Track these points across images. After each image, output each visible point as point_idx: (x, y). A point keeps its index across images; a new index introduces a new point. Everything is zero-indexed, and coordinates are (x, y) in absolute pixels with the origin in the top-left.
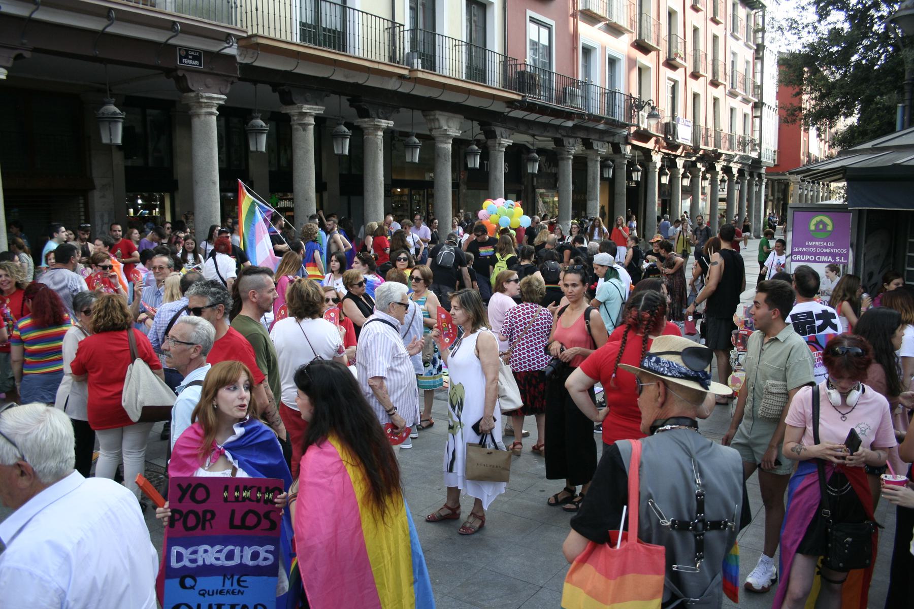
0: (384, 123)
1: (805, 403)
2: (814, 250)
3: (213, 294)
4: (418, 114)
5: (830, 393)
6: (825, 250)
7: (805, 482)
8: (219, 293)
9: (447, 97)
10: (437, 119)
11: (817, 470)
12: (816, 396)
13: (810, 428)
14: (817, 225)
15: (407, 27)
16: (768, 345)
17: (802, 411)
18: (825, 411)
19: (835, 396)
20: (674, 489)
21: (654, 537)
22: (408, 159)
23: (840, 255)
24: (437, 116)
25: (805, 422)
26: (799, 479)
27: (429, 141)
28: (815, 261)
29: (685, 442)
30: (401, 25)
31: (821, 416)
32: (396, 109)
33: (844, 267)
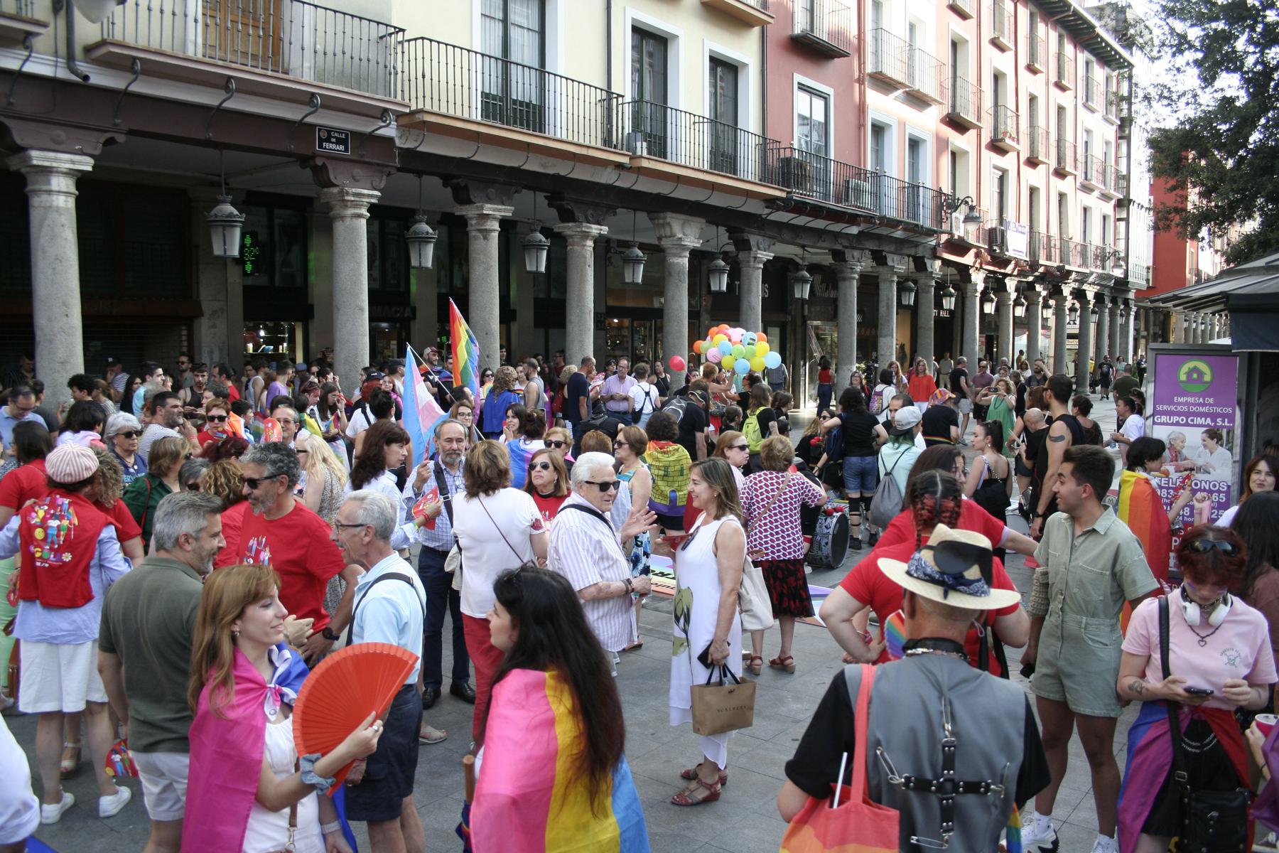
0: (595, 229)
1: (1148, 621)
2: (1185, 408)
3: (274, 462)
4: (642, 217)
5: (1185, 608)
6: (1201, 409)
7: (1151, 733)
8: (281, 461)
9: (682, 193)
10: (669, 224)
11: (1167, 716)
12: (1164, 612)
13: (1157, 656)
14: (1189, 374)
15: (628, 98)
16: (1081, 539)
17: (1145, 633)
18: (1178, 635)
19: (1193, 611)
21: (884, 797)
23: (1223, 416)
24: (668, 220)
25: (1149, 648)
27: (656, 253)
28: (1187, 425)
30: (619, 96)
31: (1171, 639)
32: (611, 210)
33: (1228, 433)
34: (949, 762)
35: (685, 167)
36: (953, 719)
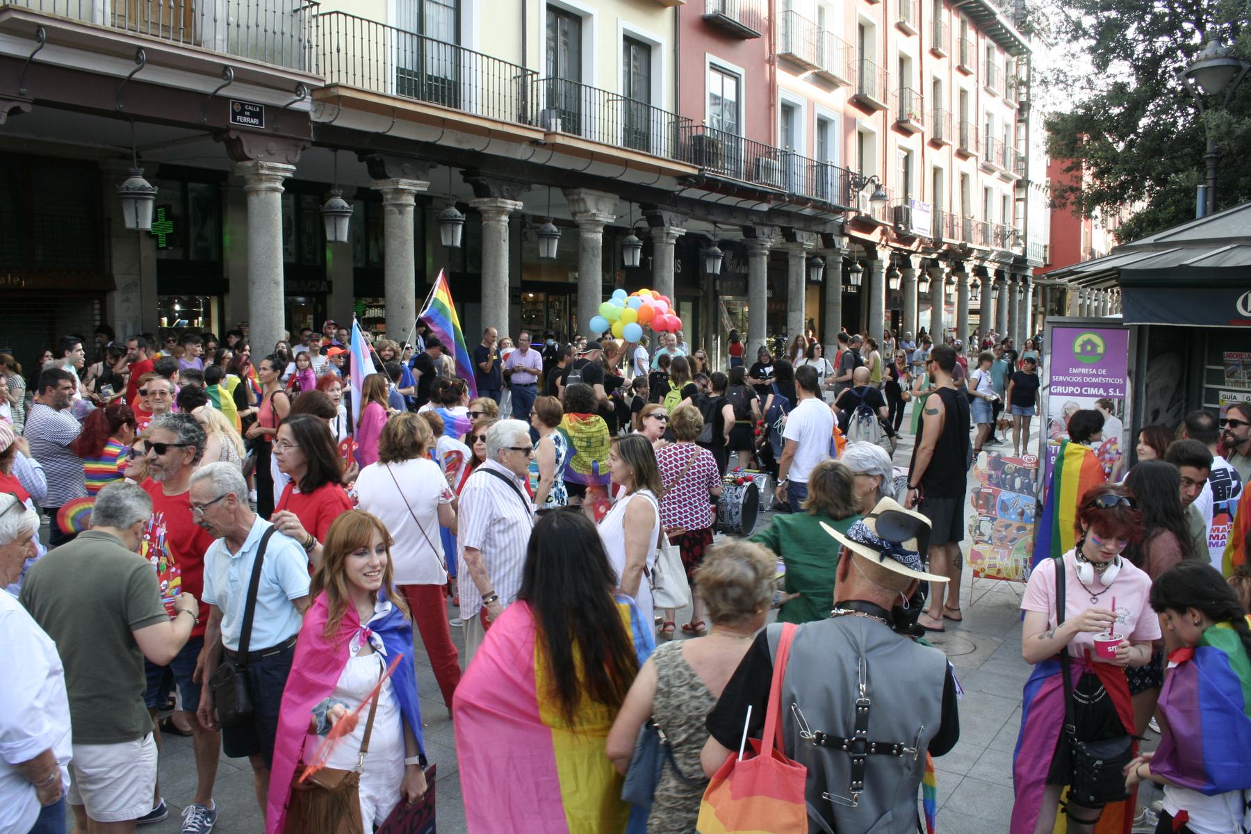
0: (510, 205)
2: (1080, 379)
4: (557, 193)
5: (1080, 568)
6: (1095, 380)
7: (1047, 688)
8: (194, 431)
10: (583, 200)
12: (1060, 572)
14: (1083, 346)
15: (543, 75)
19: (1087, 570)
20: (828, 691)
21: (796, 756)
22: (543, 254)
23: (1115, 386)
24: (583, 196)
26: (1037, 683)
27: (571, 229)
28: (1081, 395)
29: (855, 634)
30: (534, 72)
31: (1067, 598)
32: (527, 185)
33: (1119, 403)
34: (862, 722)
35: (599, 144)
36: (869, 680)
